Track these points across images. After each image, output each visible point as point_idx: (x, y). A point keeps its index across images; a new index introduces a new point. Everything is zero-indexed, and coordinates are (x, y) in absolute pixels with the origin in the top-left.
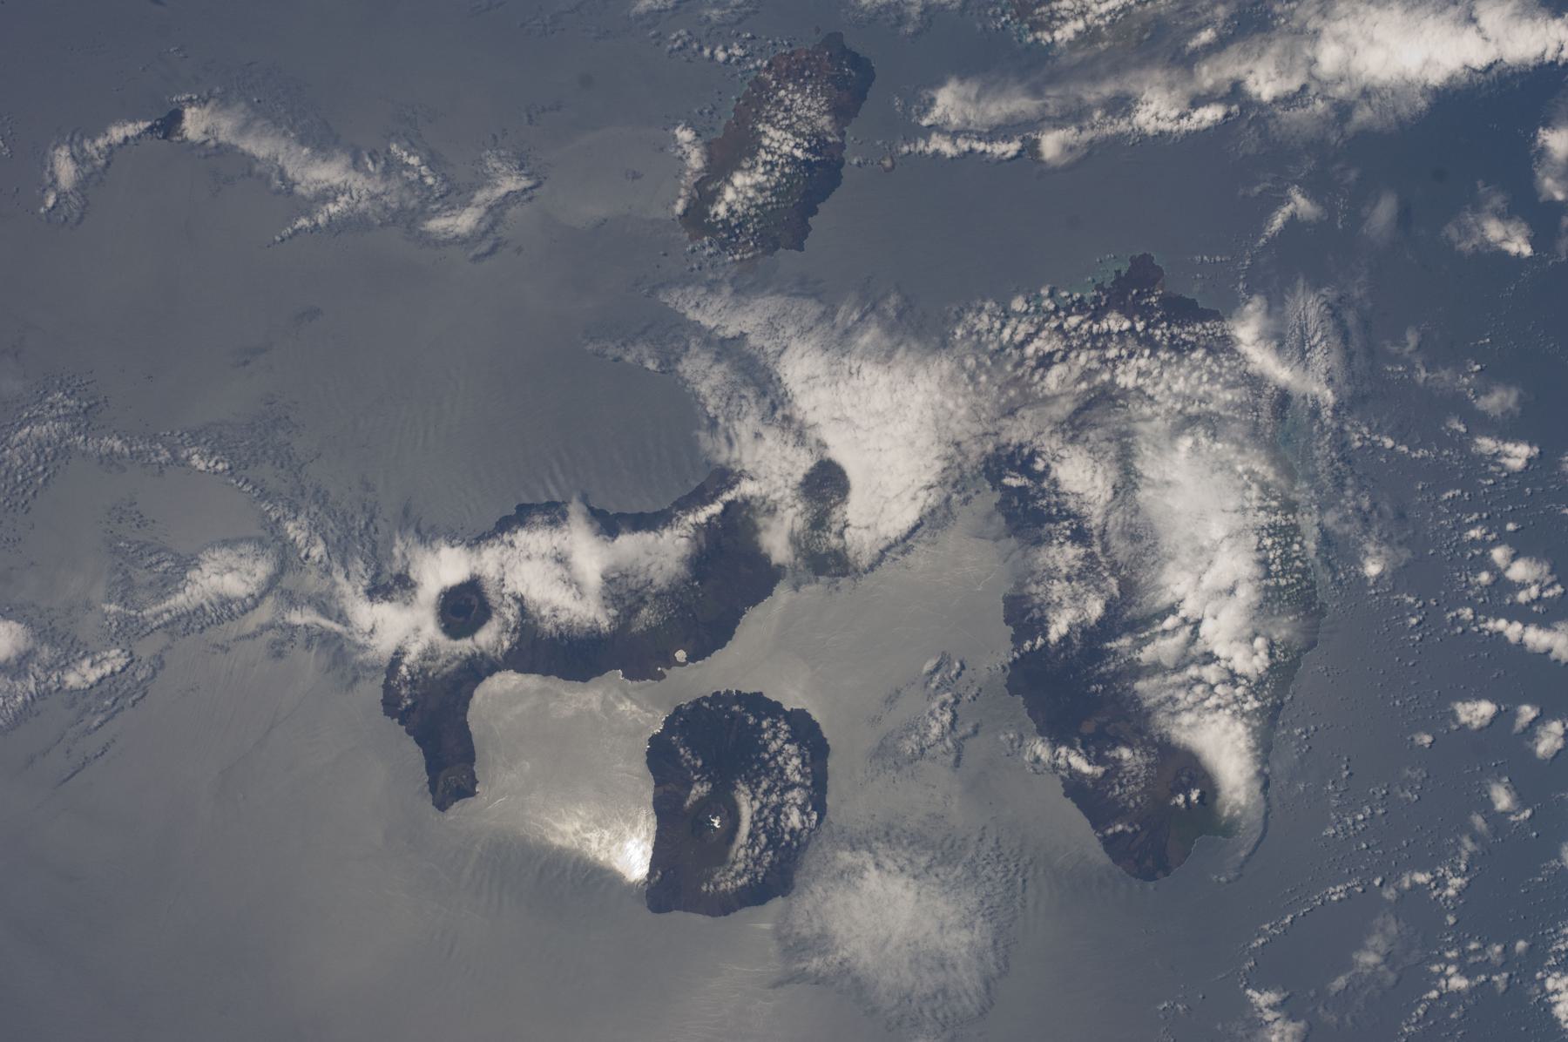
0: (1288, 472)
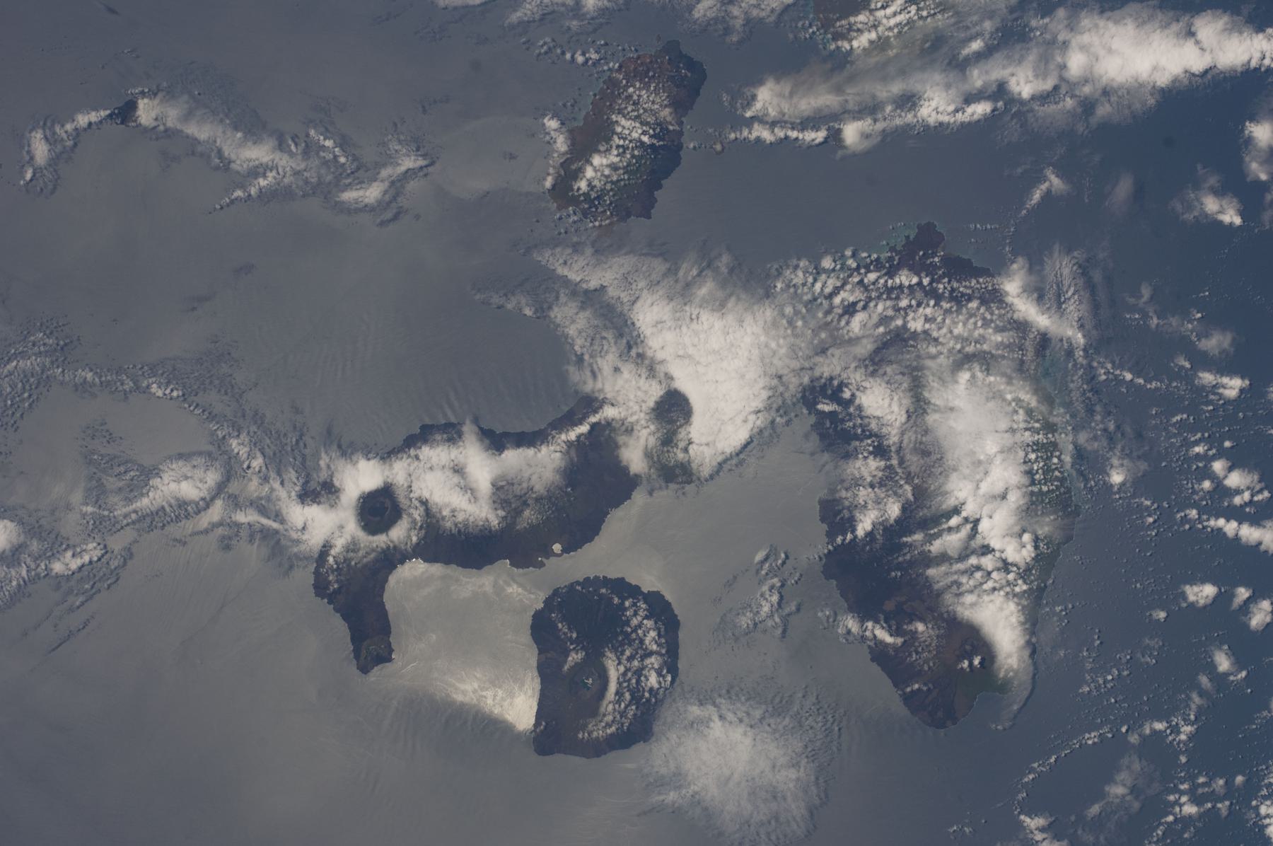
0: (1048, 400)
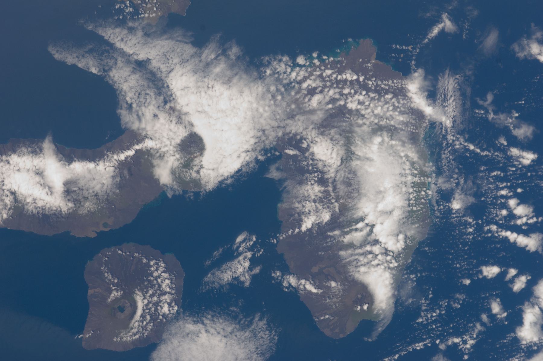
0: (422, 156)
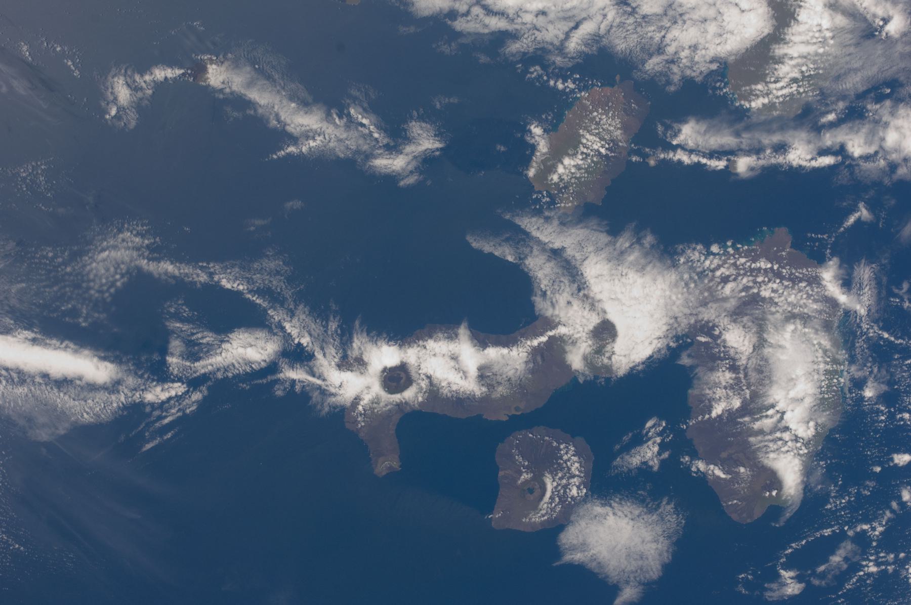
0: (835, 344)
